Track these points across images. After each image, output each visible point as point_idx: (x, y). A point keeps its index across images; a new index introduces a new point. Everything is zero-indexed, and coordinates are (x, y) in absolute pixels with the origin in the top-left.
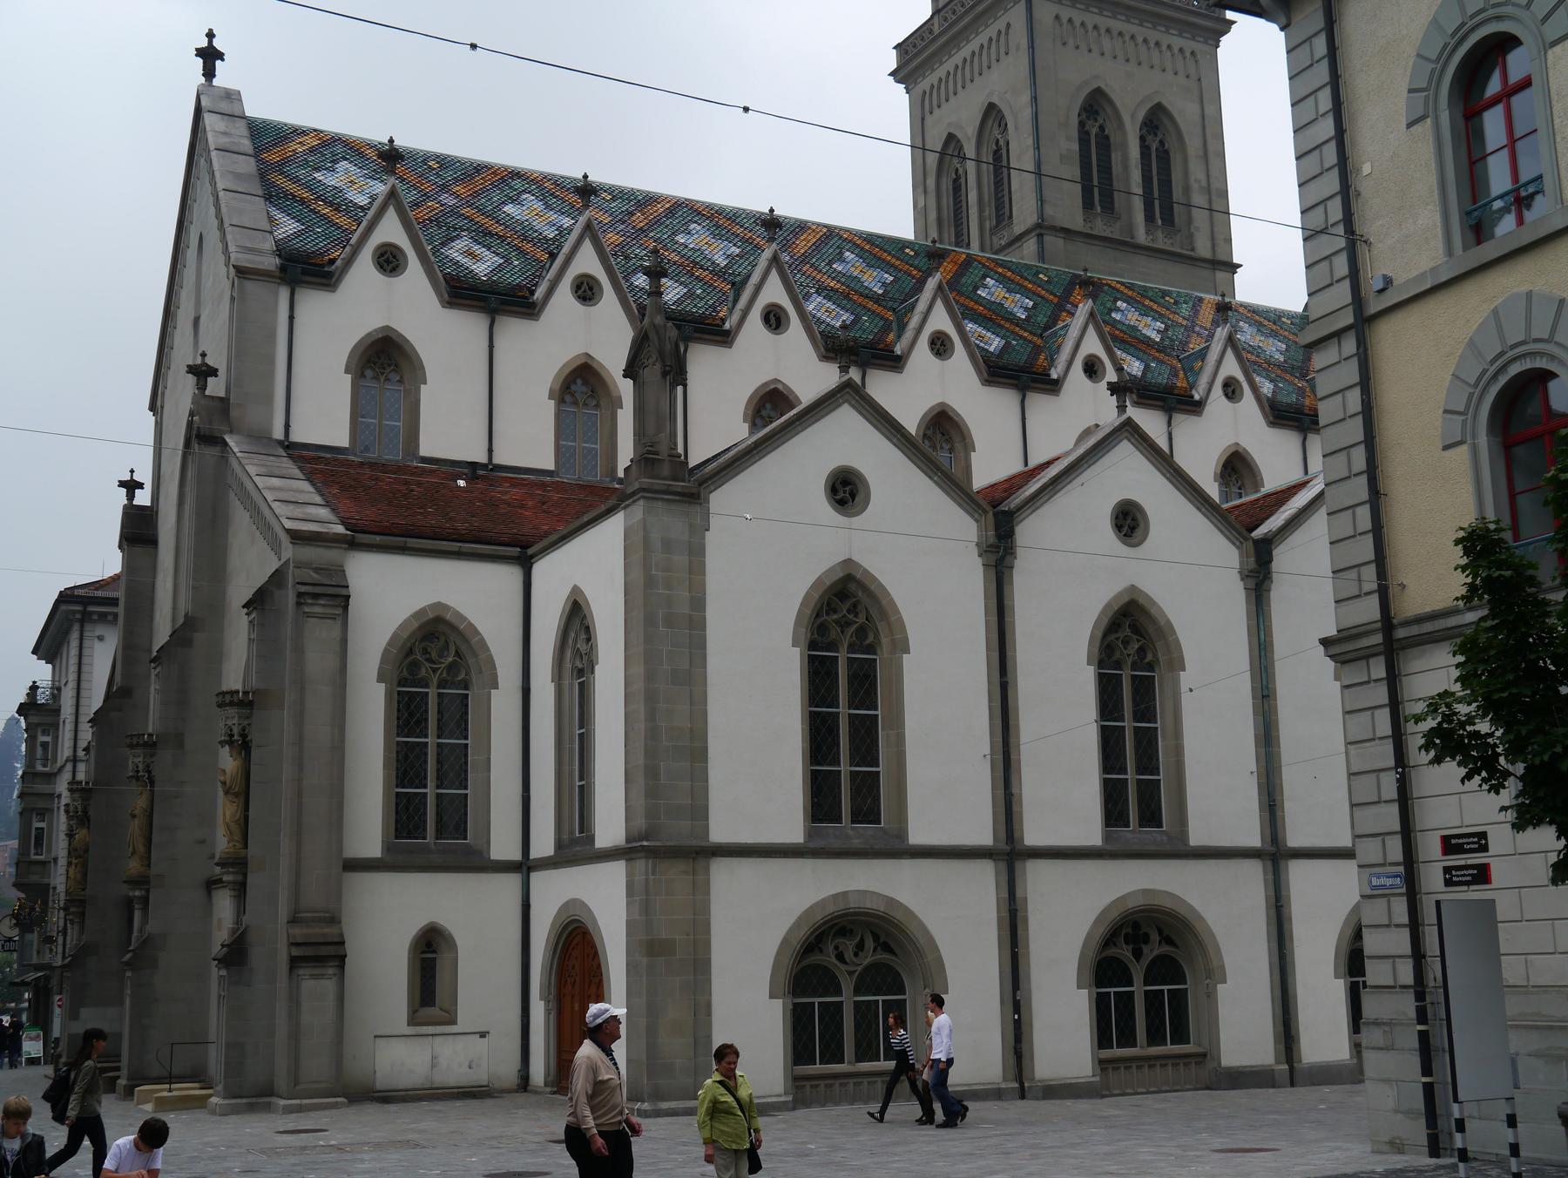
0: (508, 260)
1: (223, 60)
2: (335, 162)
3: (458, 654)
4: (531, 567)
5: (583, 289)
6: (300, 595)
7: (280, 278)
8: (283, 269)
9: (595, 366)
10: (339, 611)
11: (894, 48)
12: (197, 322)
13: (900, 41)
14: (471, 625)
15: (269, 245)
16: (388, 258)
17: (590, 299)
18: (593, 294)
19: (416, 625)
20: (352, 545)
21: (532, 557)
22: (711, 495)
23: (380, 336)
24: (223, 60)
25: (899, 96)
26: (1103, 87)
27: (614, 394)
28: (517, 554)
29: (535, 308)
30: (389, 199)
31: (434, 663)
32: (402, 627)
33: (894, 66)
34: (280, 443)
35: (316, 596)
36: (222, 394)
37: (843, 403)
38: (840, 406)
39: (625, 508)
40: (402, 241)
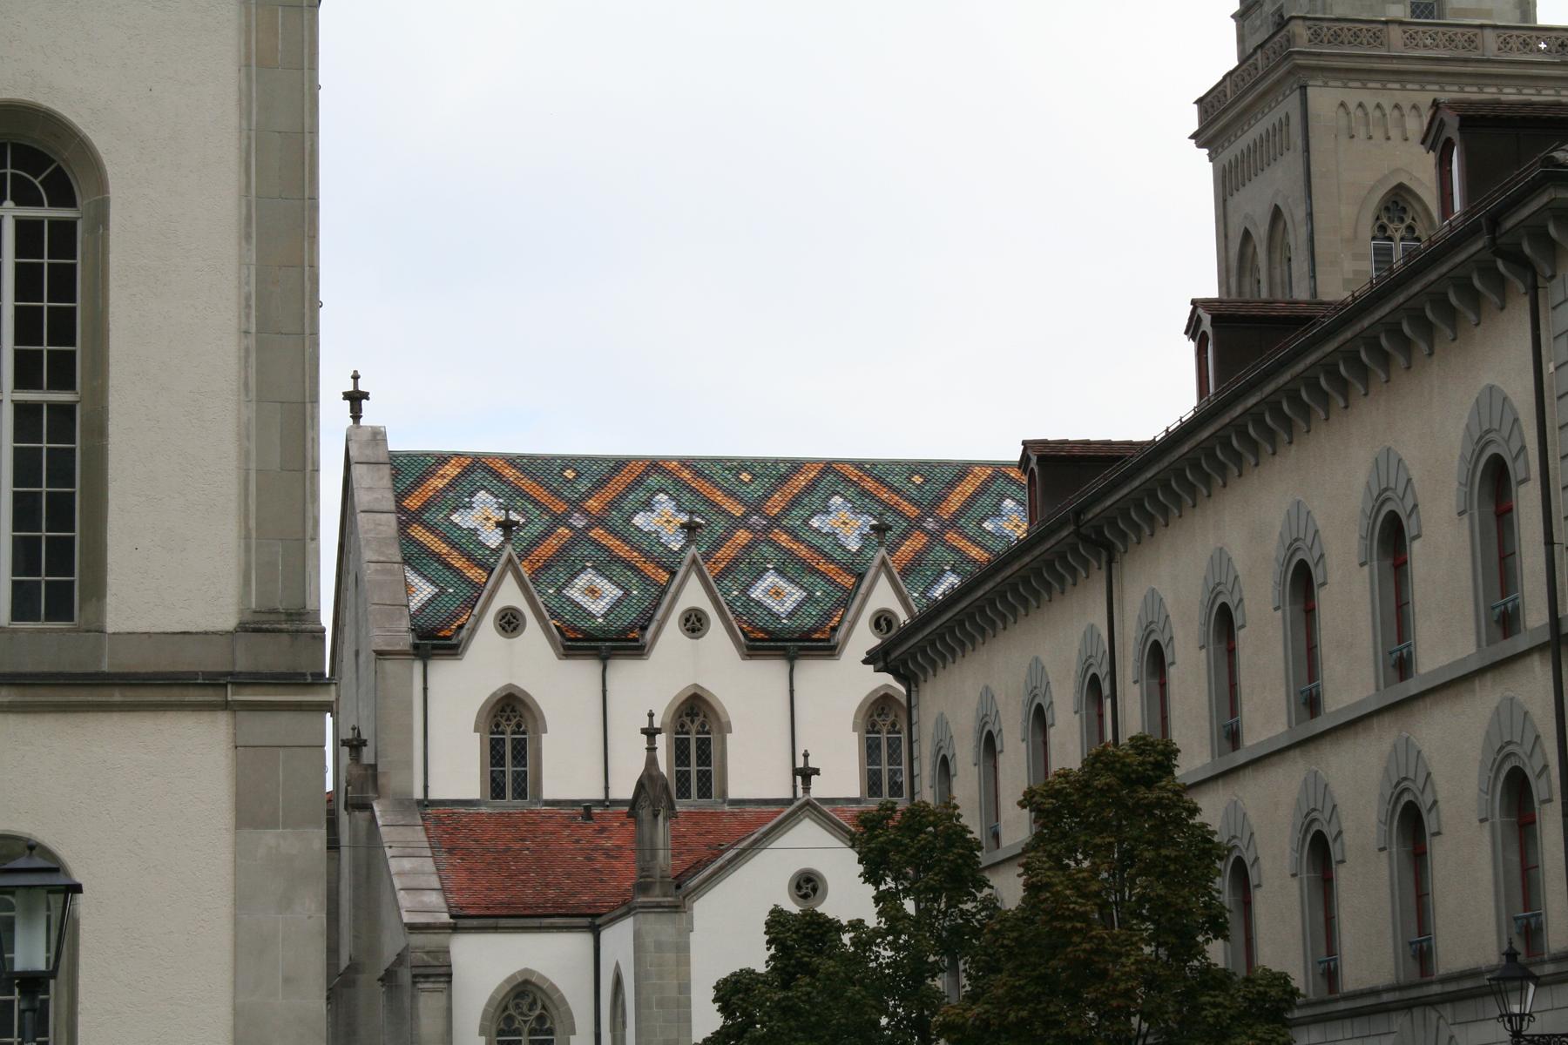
0: (627, 593)
1: (368, 399)
2: (472, 494)
3: (544, 1007)
4: (599, 934)
5: (691, 621)
6: (415, 976)
7: (414, 655)
8: (416, 647)
9: (705, 696)
10: (445, 985)
11: (1195, 103)
12: (357, 654)
13: (1202, 95)
14: (552, 985)
15: (405, 624)
16: (509, 620)
17: (699, 630)
18: (701, 625)
19: (508, 988)
20: (455, 929)
21: (600, 926)
22: (695, 904)
23: (504, 694)
24: (368, 399)
25: (1199, 168)
26: (1407, 182)
27: (723, 720)
28: (588, 924)
29: (644, 649)
30: (507, 566)
31: (526, 1015)
32: (497, 991)
33: (1195, 127)
34: (419, 802)
35: (427, 976)
36: (373, 762)
37: (804, 818)
38: (801, 820)
39: (634, 915)
40: (520, 603)
